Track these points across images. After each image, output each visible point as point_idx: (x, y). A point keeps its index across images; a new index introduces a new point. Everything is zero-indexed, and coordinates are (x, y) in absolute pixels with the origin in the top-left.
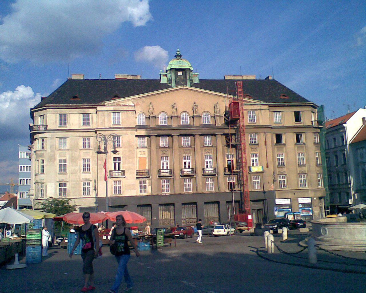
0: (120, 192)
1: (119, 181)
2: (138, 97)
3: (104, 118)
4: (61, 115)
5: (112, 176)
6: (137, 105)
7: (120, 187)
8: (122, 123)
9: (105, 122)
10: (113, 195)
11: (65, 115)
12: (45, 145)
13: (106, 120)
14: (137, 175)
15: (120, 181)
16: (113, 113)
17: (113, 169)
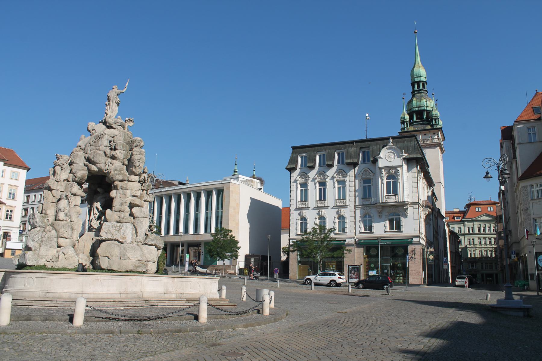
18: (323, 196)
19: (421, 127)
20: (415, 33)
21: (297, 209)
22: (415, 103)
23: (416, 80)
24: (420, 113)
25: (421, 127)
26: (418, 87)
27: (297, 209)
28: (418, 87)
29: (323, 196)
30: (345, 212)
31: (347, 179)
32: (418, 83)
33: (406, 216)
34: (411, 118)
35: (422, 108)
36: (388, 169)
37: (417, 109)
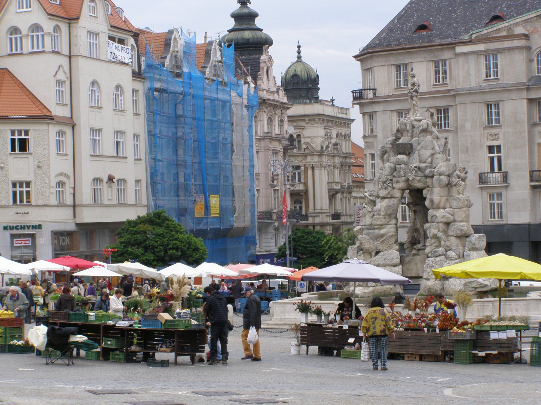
0: (501, 215)
1: (500, 195)
2: (533, 15)
3: (469, 67)
4: (398, 67)
5: (486, 183)
6: (533, 32)
7: (500, 206)
8: (502, 75)
9: (469, 75)
10: (489, 221)
11: (406, 66)
12: (374, 127)
13: (473, 71)
14: (531, 180)
15: (501, 194)
16: (486, 54)
17: (488, 169)
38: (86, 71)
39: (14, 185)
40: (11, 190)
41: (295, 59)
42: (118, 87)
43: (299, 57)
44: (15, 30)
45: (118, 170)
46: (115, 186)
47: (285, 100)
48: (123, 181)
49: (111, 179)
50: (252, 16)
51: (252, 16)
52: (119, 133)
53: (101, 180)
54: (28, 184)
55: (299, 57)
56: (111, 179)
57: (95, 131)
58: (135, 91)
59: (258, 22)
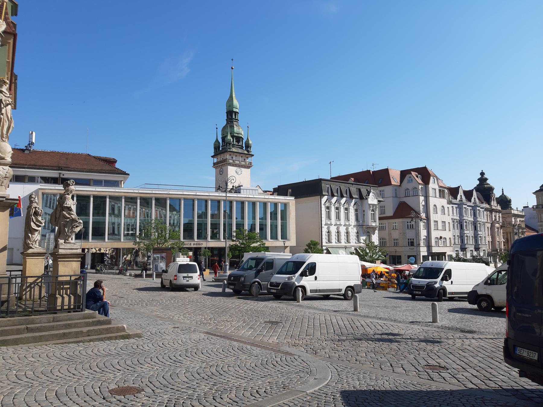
18: (338, 217)
19: (240, 151)
20: (232, 68)
21: (325, 225)
22: (236, 129)
23: (235, 110)
24: (239, 139)
25: (240, 151)
26: (235, 116)
27: (325, 225)
28: (235, 116)
29: (338, 217)
30: (350, 229)
31: (350, 207)
32: (236, 113)
33: (374, 234)
34: (233, 141)
35: (240, 135)
36: (373, 205)
37: (237, 135)
38: (433, 201)
39: (409, 239)
40: (407, 241)
41: (501, 194)
42: (443, 206)
43: (503, 193)
44: (408, 189)
45: (444, 234)
46: (442, 240)
47: (500, 209)
48: (445, 238)
49: (441, 238)
50: (486, 179)
51: (486, 179)
52: (444, 222)
53: (437, 238)
54: (413, 240)
55: (503, 193)
56: (441, 238)
57: (436, 222)
58: (448, 208)
59: (488, 182)
